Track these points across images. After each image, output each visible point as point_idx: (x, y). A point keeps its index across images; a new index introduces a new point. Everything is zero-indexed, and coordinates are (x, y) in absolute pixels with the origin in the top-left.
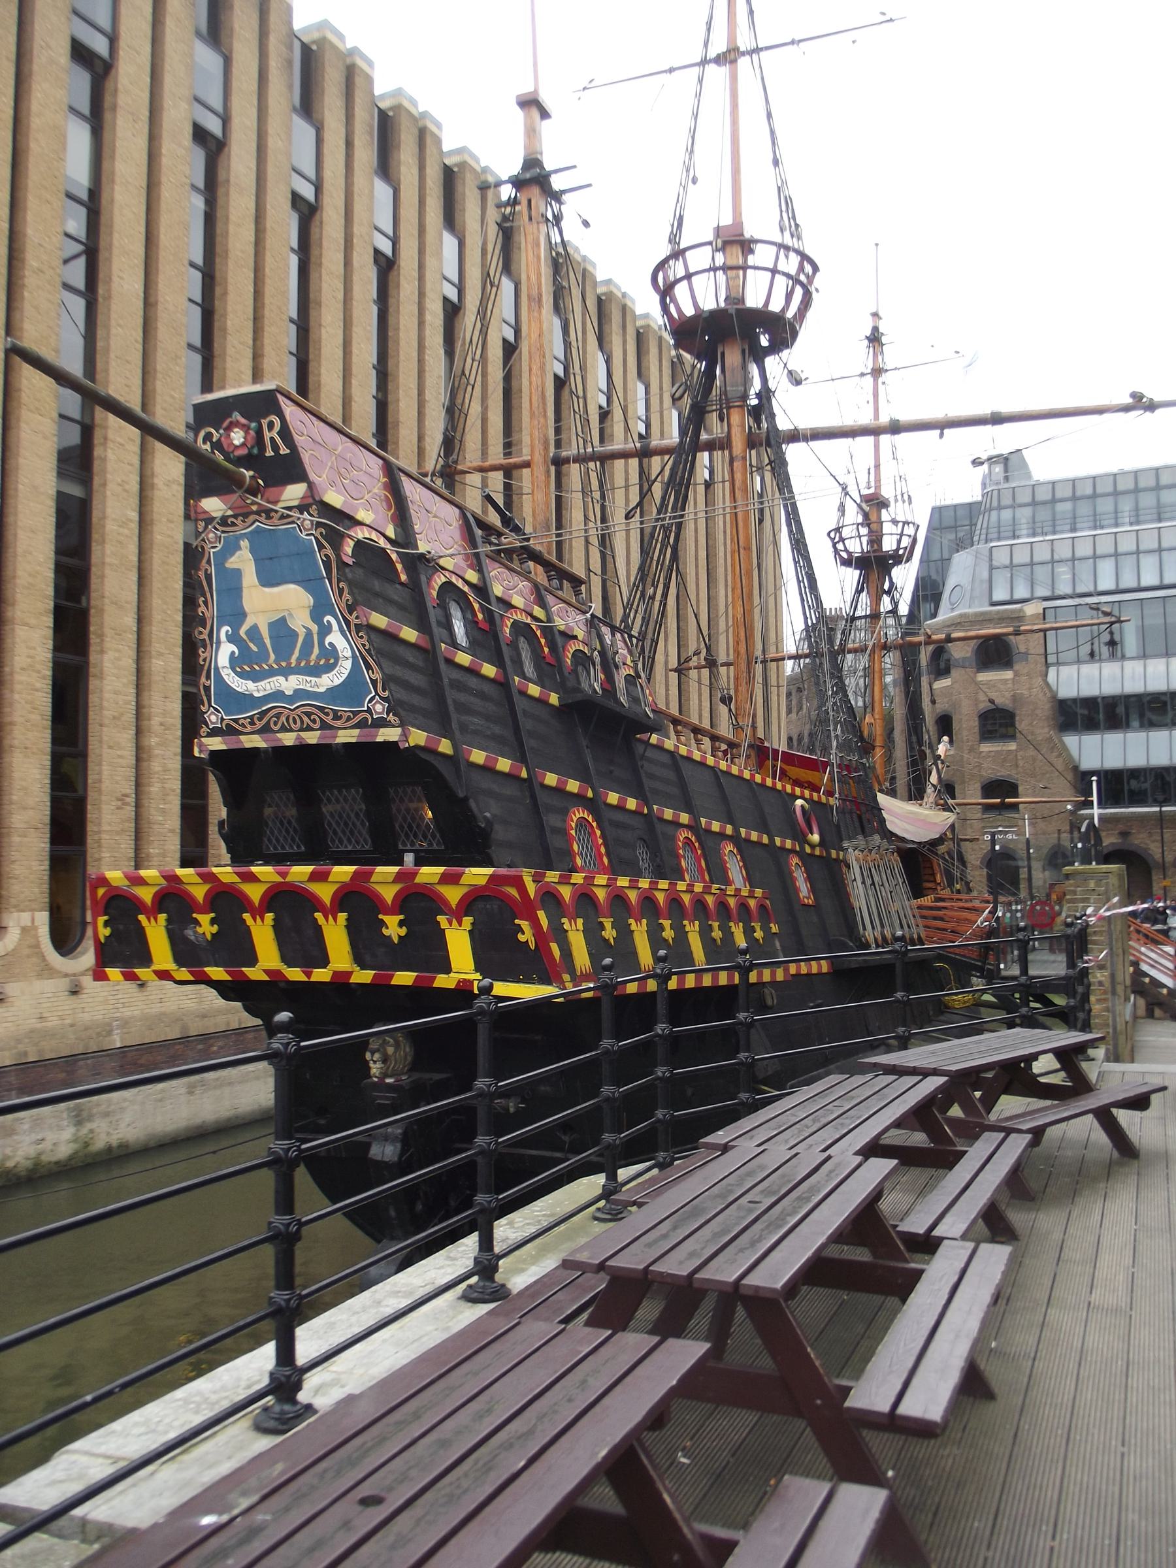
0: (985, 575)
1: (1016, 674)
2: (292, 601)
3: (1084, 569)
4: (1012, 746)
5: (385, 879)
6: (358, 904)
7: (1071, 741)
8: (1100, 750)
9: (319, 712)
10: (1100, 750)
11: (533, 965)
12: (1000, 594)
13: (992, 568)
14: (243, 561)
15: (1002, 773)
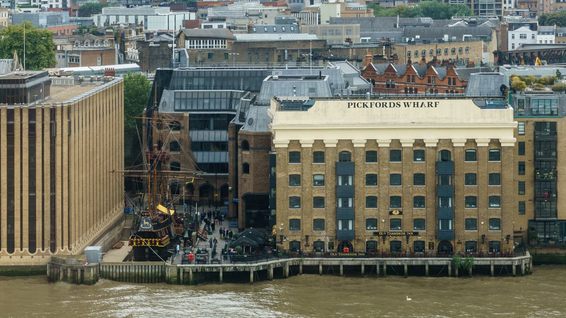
0: (173, 100)
1: (181, 132)
2: (148, 223)
3: (201, 102)
4: (179, 153)
5: (153, 240)
6: (151, 241)
7: (195, 153)
8: (202, 157)
9: (148, 229)
10: (202, 157)
11: (163, 245)
12: (177, 107)
13: (175, 98)
14: (144, 221)
15: (177, 160)
